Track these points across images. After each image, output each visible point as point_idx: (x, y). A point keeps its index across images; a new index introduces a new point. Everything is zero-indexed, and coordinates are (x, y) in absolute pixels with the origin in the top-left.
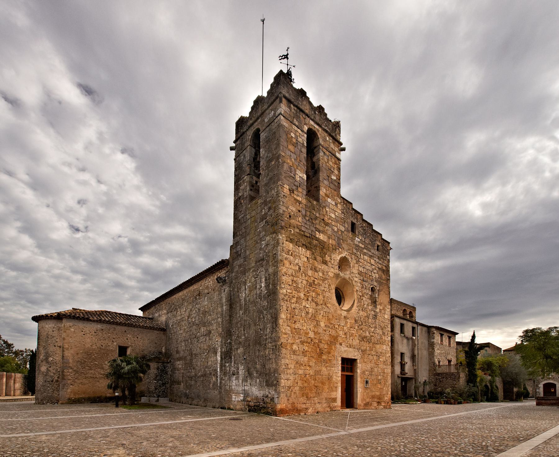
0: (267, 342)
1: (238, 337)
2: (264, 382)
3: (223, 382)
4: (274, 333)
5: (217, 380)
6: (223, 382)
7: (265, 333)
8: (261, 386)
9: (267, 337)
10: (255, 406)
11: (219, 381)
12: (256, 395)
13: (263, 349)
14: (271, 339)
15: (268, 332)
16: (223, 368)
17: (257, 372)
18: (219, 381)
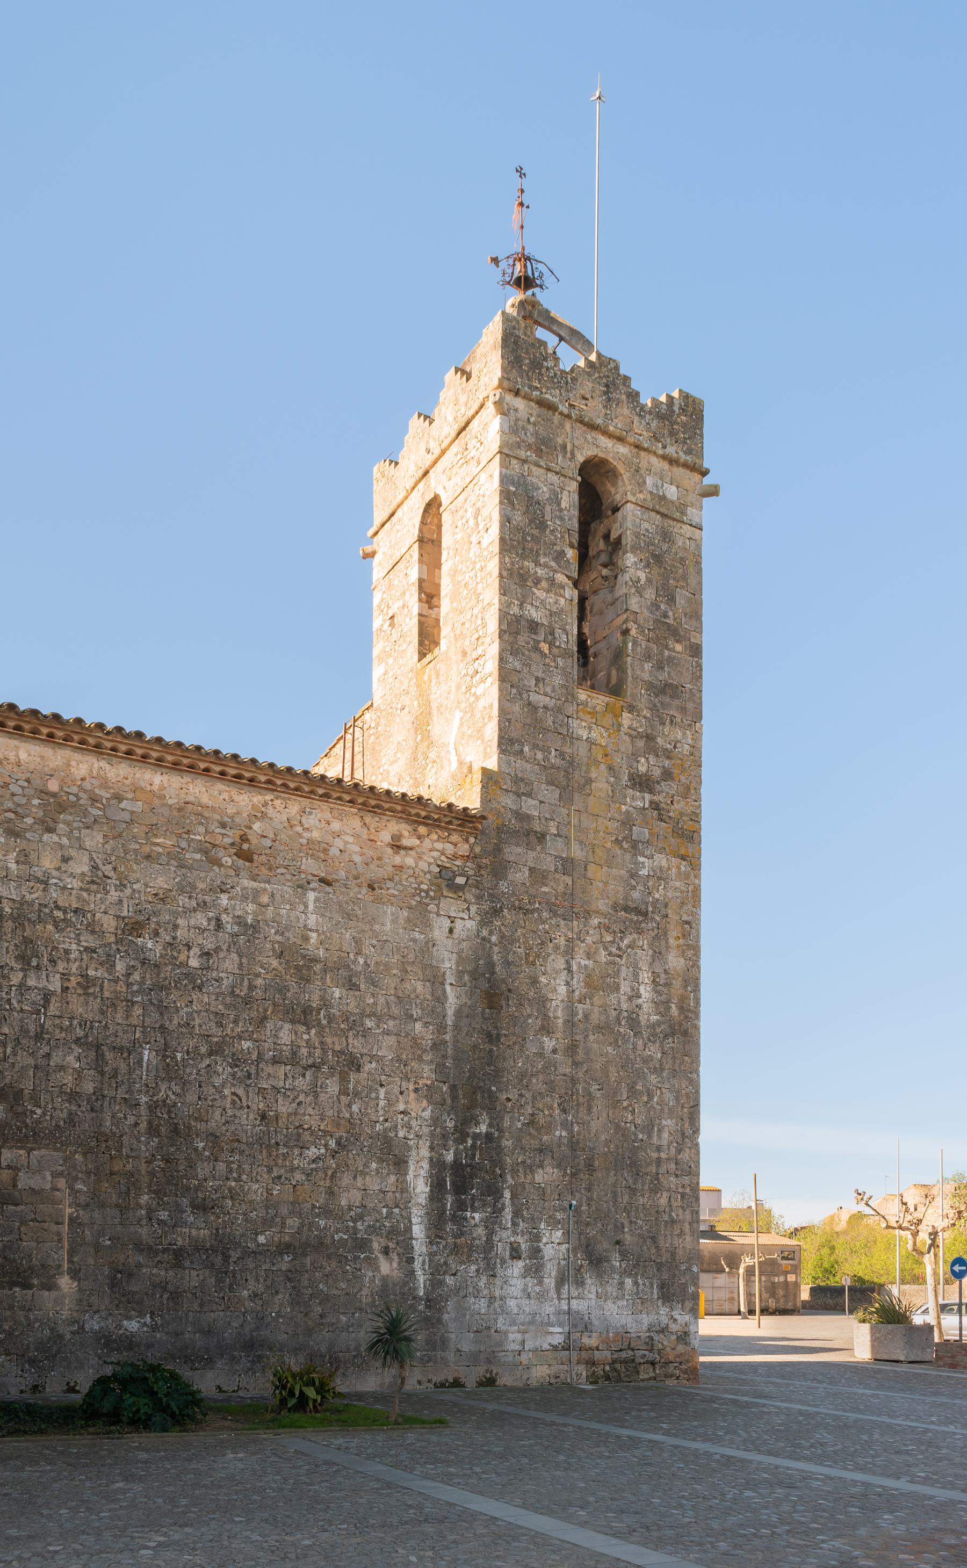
0: (663, 1170)
1: (532, 1123)
2: (652, 1286)
3: (449, 1280)
4: (687, 1150)
5: (413, 1272)
6: (449, 1280)
7: (655, 1140)
8: (640, 1301)
9: (663, 1155)
10: (614, 1362)
11: (421, 1279)
12: (623, 1327)
13: (646, 1187)
14: (676, 1164)
15: (664, 1142)
16: (449, 1227)
17: (624, 1255)
18: (421, 1279)
